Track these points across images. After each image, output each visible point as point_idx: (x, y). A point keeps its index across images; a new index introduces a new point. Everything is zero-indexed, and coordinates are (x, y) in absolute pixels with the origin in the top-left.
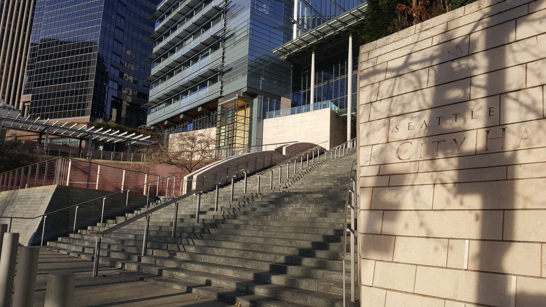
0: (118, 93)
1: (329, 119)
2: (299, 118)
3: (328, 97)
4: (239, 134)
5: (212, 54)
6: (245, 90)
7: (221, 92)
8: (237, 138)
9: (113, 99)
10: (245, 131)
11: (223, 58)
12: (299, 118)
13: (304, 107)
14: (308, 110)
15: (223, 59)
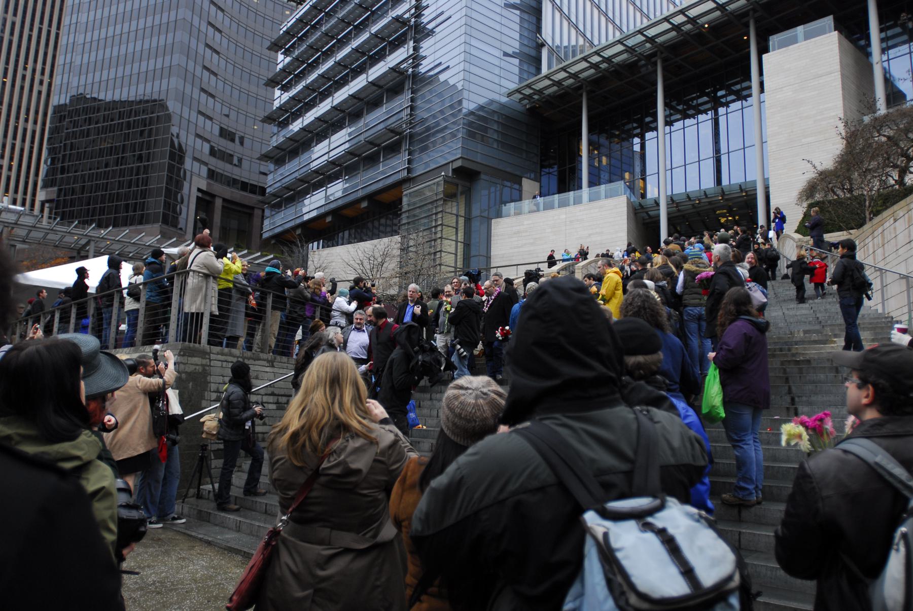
0: (208, 184)
1: (626, 217)
2: (563, 216)
3: (614, 175)
4: (449, 246)
5: (388, 104)
6: (459, 164)
7: (409, 170)
8: (443, 254)
9: (200, 195)
10: (457, 241)
11: (412, 108)
12: (563, 216)
13: (571, 194)
14: (578, 201)
15: (411, 110)
